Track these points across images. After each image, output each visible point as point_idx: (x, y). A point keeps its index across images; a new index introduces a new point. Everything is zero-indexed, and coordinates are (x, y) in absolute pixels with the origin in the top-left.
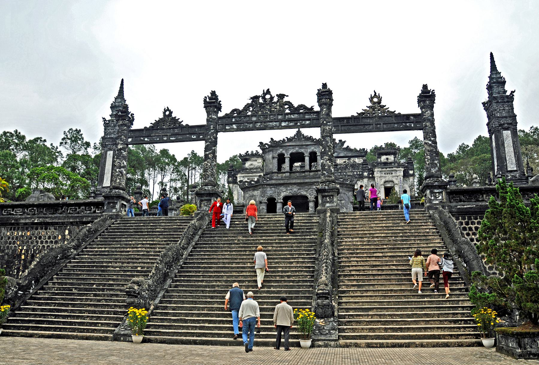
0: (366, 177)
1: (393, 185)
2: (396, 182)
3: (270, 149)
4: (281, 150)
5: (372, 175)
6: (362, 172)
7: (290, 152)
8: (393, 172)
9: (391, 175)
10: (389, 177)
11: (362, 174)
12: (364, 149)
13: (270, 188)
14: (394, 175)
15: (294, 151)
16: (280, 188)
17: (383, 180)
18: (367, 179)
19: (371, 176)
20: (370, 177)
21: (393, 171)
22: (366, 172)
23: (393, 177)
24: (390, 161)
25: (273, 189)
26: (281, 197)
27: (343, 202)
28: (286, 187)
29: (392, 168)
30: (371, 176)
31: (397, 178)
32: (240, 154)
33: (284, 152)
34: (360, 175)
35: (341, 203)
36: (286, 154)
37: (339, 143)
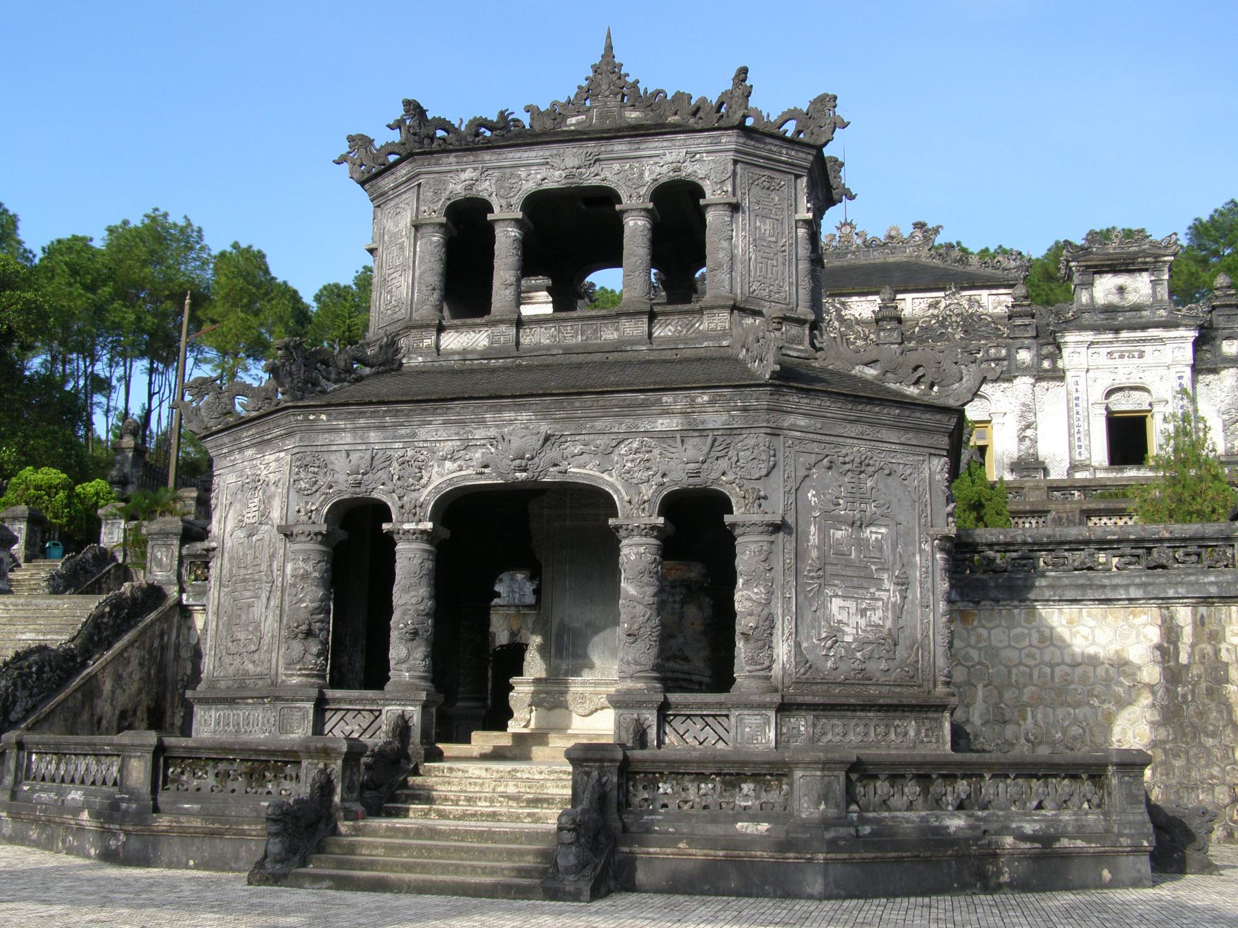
0: (1024, 370)
3: (403, 171)
4: (468, 174)
5: (1054, 362)
7: (529, 186)
8: (1148, 349)
9: (1136, 361)
10: (1126, 372)
13: (354, 430)
15: (554, 179)
16: (423, 433)
17: (1106, 382)
19: (1046, 364)
24: (1132, 298)
25: (373, 436)
26: (427, 495)
27: (873, 534)
28: (462, 423)
29: (1144, 327)
30: (1046, 364)
33: (486, 189)
35: (862, 544)
36: (495, 203)
37: (912, 236)
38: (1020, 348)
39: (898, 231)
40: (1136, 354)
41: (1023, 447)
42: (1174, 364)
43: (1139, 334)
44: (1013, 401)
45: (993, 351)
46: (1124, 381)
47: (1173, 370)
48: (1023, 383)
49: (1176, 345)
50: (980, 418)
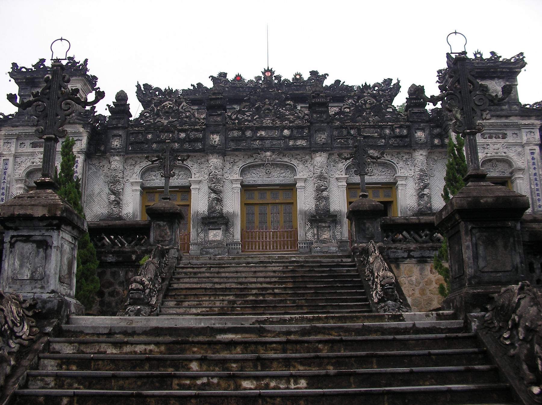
0: (422, 146)
1: (507, 174)
2: (519, 162)
5: (442, 140)
6: (408, 128)
8: (509, 133)
9: (501, 140)
11: (410, 135)
12: (392, 80)
14: (510, 139)
18: (424, 153)
19: (436, 141)
20: (436, 146)
21: (507, 126)
22: (423, 130)
23: (509, 146)
29: (507, 117)
30: (436, 141)
31: (520, 149)
32: (14, 65)
34: (402, 137)
38: (418, 129)
39: (300, 75)
40: (500, 136)
41: (422, 203)
42: (528, 144)
43: (504, 120)
44: (413, 168)
45: (398, 130)
46: (494, 154)
47: (527, 148)
48: (420, 156)
49: (528, 130)
50: (387, 180)
